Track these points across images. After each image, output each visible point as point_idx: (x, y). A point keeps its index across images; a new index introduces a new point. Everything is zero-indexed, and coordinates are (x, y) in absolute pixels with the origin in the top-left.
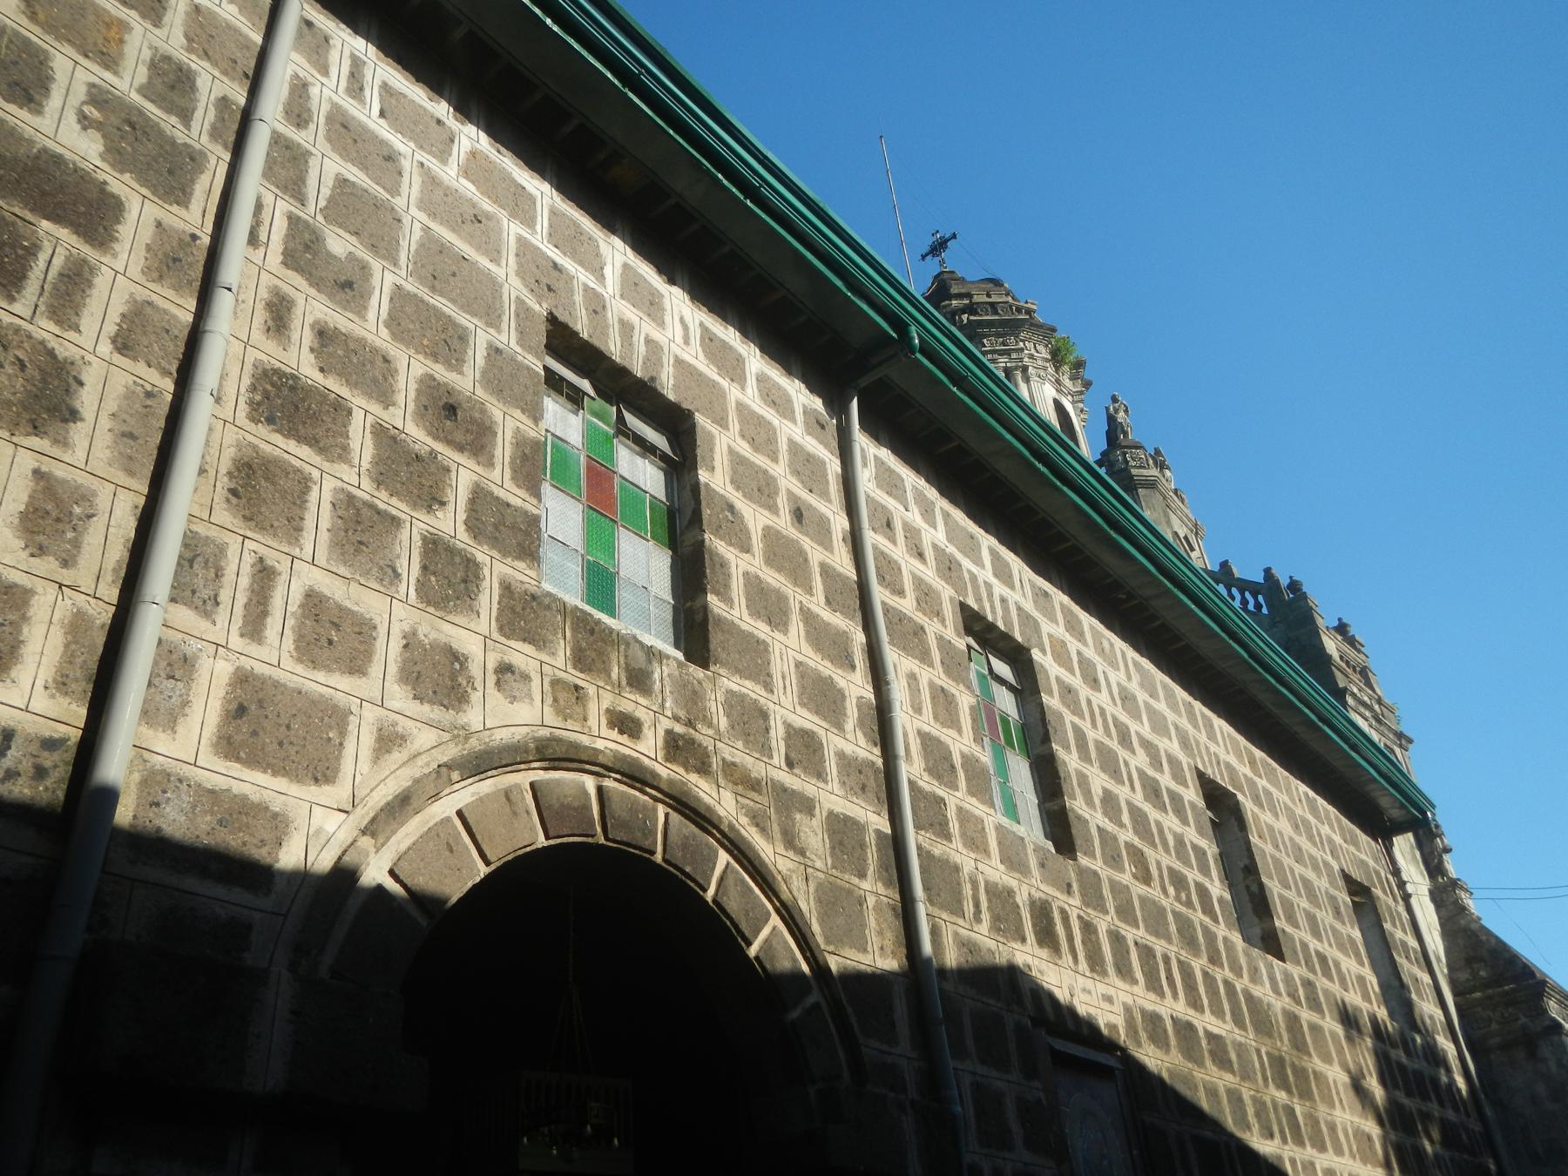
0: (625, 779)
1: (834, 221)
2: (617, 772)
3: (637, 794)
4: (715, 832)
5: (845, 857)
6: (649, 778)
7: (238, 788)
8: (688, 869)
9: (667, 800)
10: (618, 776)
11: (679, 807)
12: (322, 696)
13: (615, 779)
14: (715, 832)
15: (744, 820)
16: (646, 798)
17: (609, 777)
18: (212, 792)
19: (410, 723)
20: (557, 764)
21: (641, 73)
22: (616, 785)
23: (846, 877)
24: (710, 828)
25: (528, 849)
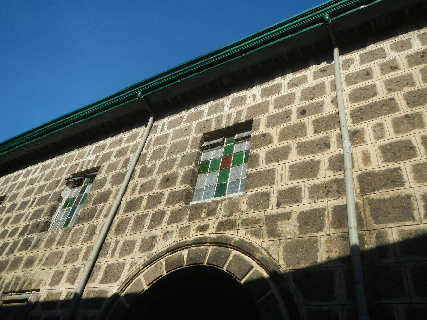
0: (197, 245)
1: (268, 29)
2: (193, 244)
3: (203, 247)
4: (230, 246)
5: (309, 227)
6: (203, 241)
7: (101, 289)
8: (214, 263)
9: (212, 244)
10: (195, 245)
11: (216, 244)
12: (121, 262)
13: (194, 246)
14: (230, 246)
15: (248, 236)
16: (206, 247)
17: (192, 247)
18: (97, 291)
19: (138, 259)
20: (174, 251)
21: (198, 67)
22: (195, 248)
23: (308, 235)
24: (226, 245)
25: (161, 278)
